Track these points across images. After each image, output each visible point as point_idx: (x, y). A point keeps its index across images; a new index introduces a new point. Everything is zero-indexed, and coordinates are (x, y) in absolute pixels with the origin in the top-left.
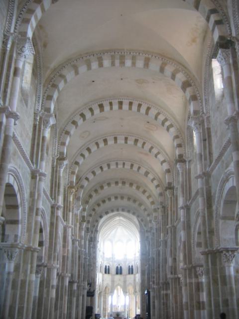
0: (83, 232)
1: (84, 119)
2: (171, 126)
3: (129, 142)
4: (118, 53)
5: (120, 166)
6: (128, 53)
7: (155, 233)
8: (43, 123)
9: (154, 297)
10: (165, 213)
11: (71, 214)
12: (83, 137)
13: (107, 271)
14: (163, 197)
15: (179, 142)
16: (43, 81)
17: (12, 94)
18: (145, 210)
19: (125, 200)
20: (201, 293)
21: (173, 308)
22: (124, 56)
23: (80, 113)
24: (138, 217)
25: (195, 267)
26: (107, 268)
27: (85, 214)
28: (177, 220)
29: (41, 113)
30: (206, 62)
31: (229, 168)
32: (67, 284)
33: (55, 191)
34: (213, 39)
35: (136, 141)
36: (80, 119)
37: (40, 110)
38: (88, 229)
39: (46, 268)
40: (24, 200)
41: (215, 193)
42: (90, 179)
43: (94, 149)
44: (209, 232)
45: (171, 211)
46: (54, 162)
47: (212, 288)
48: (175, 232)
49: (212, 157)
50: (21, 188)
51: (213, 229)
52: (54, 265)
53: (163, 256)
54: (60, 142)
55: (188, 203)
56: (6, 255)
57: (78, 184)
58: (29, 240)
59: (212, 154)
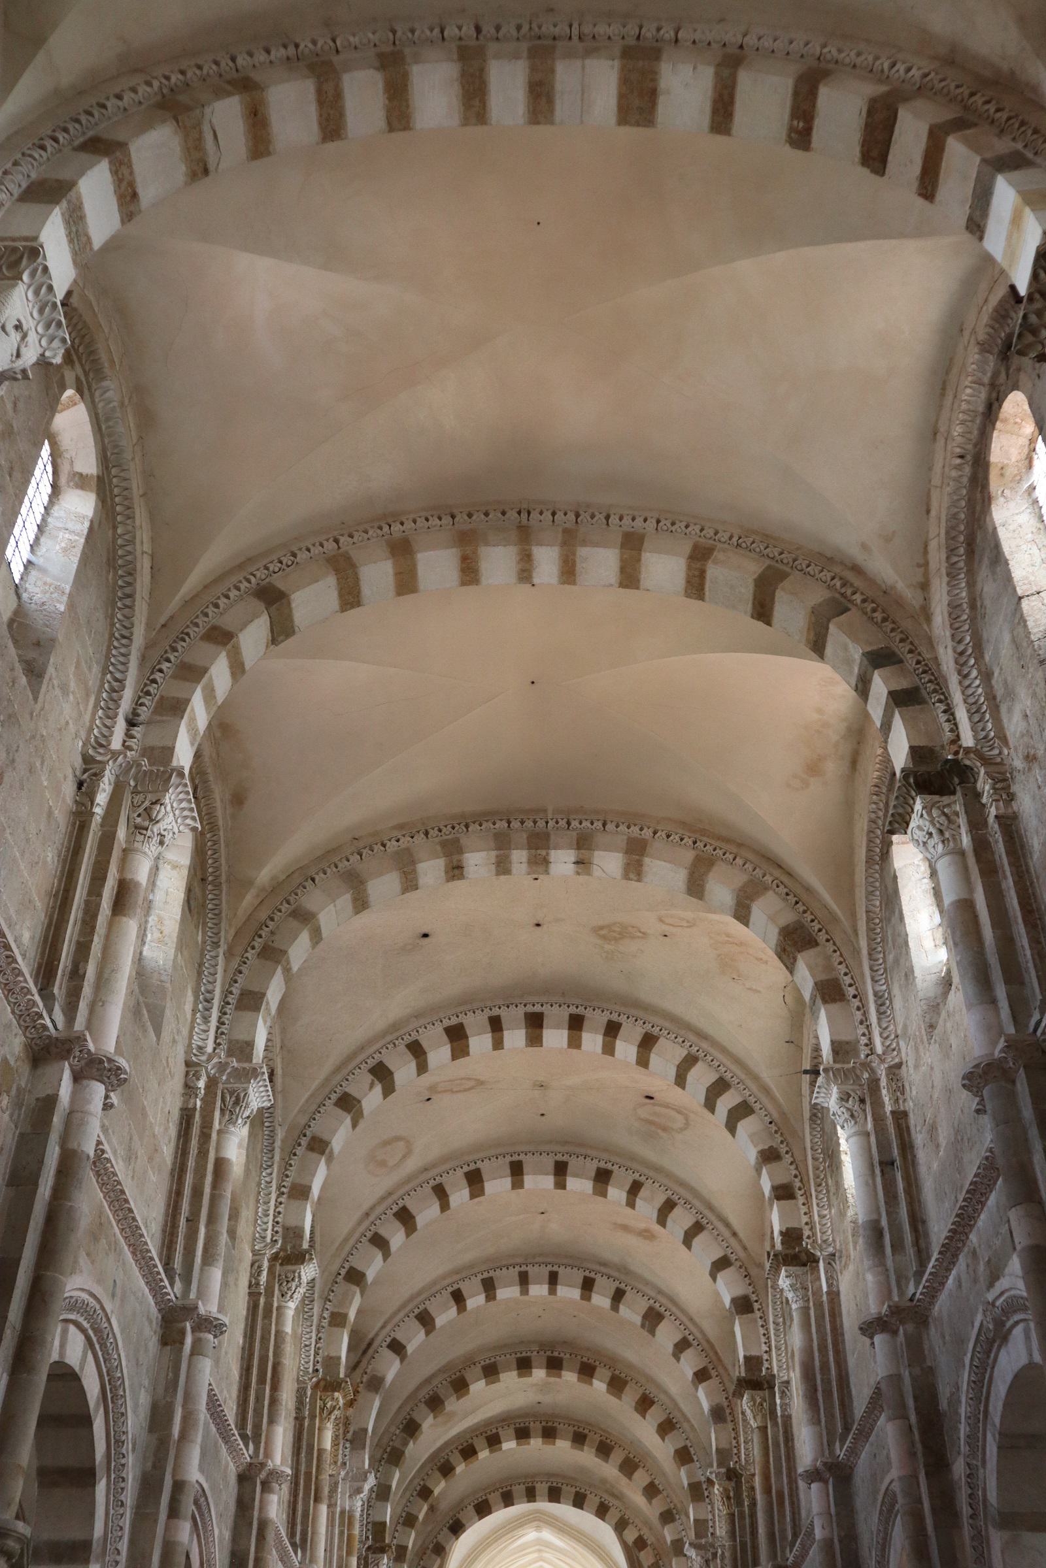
1: (389, 1090)
3: (572, 1183)
4: (522, 822)
5: (538, 1290)
6: (563, 823)
10: (740, 1503)
11: (323, 1509)
12: (383, 1164)
14: (730, 1426)
15: (782, 1179)
16: (227, 934)
17: (103, 983)
18: (651, 1491)
19: (563, 1446)
22: (547, 836)
23: (372, 1063)
24: (620, 1527)
27: (388, 1514)
28: (795, 1535)
29: (215, 1060)
30: (869, 850)
31: (1003, 1283)
33: (259, 1399)
34: (887, 760)
35: (602, 1177)
36: (372, 1086)
37: (209, 1049)
40: (120, 1443)
41: (954, 1401)
42: (410, 1349)
45: (767, 1490)
46: (259, 1275)
49: (927, 1235)
50: (114, 1389)
55: (841, 1452)
57: (359, 1371)
59: (924, 1222)
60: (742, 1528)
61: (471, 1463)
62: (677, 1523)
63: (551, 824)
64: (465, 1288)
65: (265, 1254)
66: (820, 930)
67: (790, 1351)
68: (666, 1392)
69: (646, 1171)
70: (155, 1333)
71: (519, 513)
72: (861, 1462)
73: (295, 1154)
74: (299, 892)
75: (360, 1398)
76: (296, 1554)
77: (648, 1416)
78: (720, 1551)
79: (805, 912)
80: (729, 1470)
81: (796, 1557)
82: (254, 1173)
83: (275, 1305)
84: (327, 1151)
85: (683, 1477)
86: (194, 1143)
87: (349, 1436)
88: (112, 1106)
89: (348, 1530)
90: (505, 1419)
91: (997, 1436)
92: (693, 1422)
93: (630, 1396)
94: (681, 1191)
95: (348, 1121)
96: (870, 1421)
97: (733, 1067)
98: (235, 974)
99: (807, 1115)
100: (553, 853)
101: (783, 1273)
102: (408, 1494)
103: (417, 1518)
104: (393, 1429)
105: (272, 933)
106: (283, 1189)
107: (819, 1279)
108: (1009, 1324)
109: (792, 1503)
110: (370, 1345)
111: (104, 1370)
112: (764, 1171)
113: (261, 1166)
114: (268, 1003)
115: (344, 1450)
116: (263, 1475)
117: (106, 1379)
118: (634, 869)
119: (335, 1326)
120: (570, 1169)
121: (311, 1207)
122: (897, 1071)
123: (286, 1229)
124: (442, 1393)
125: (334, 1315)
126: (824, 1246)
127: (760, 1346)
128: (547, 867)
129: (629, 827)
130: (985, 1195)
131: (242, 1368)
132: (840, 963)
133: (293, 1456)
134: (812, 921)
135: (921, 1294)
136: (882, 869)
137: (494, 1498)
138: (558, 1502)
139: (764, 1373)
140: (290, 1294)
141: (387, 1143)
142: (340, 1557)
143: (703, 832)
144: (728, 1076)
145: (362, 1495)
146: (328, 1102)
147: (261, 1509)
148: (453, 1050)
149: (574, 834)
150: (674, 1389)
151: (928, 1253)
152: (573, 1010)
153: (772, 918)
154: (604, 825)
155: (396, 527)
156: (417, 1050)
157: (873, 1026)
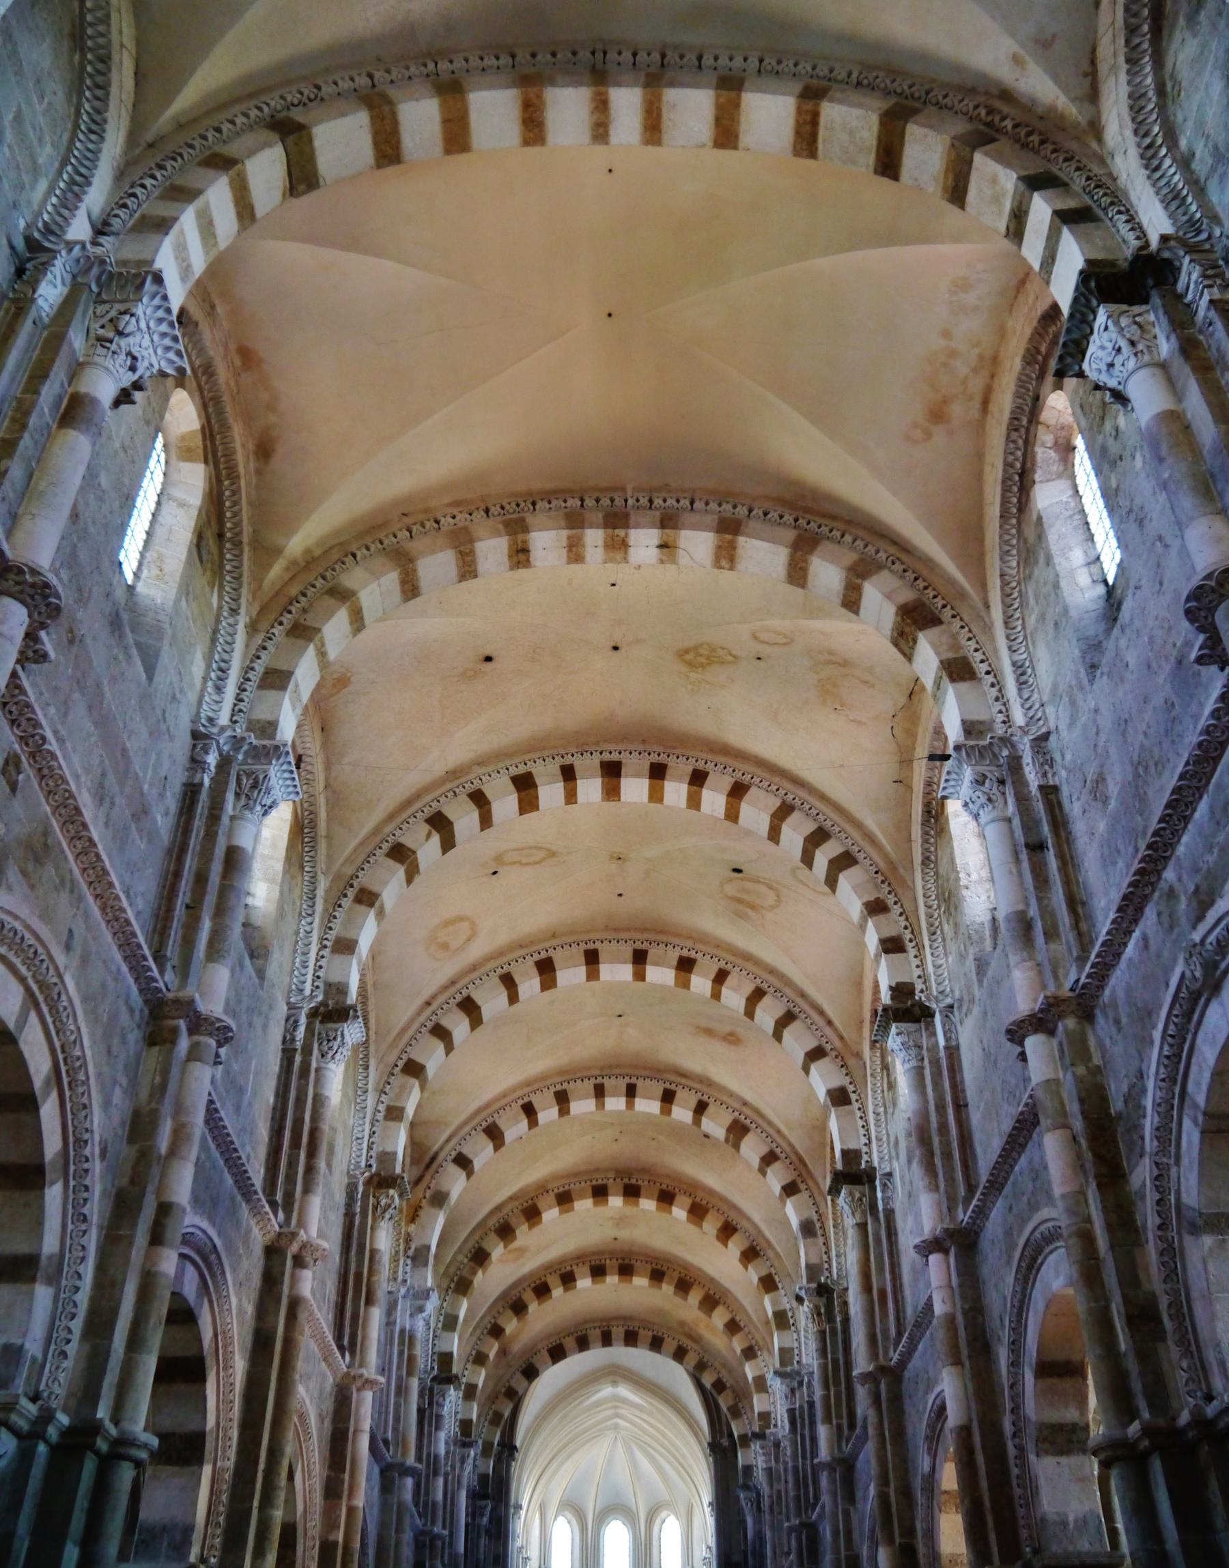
1: (448, 844)
2: (844, 861)
4: (598, 500)
5: (616, 1103)
6: (644, 501)
7: (786, 1444)
8: (232, 785)
10: (831, 1319)
14: (821, 1240)
15: (891, 932)
18: (733, 1327)
19: (640, 1281)
23: (428, 812)
28: (900, 1334)
33: (292, 1164)
35: (685, 965)
36: (429, 836)
38: (466, 1425)
40: (81, 1143)
41: (1134, 1096)
42: (477, 1164)
43: (492, 1002)
44: (1131, 1321)
45: (867, 1287)
48: (897, 1399)
49: (1090, 917)
51: (1152, 1300)
53: (836, 1551)
54: (332, 935)
55: (963, 1216)
60: (834, 1344)
61: (544, 1301)
62: (760, 1358)
63: (630, 502)
64: (536, 1100)
65: (301, 1008)
66: (944, 606)
67: (892, 1139)
68: (749, 1219)
69: (732, 959)
70: (139, 1026)
71: (593, 53)
72: (989, 1225)
73: (340, 906)
74: (337, 567)
75: (422, 1213)
77: (730, 1244)
78: (806, 1379)
79: (926, 588)
83: (314, 1065)
84: (377, 904)
86: (198, 823)
87: (410, 1253)
88: (43, 657)
89: (409, 1349)
90: (580, 1258)
91: (1200, 1118)
93: (711, 1225)
94: (772, 980)
95: (400, 872)
96: (1006, 1167)
97: (835, 817)
98: (257, 650)
99: (918, 859)
100: (633, 533)
102: (478, 1332)
104: (460, 1257)
105: (304, 611)
106: (325, 942)
107: (934, 1034)
109: (896, 1301)
110: (433, 1159)
111: (57, 1044)
112: (870, 924)
113: (300, 914)
114: (297, 686)
116: (294, 1248)
117: (61, 1057)
118: (726, 556)
120: (648, 960)
121: (359, 964)
122: (1043, 744)
123: (329, 985)
124: (513, 1222)
125: (390, 1109)
126: (941, 997)
127: (859, 1138)
128: (626, 553)
129: (720, 505)
130: (1192, 805)
131: (272, 1129)
132: (970, 639)
133: (342, 1253)
134: (935, 597)
135: (1088, 976)
136: (1019, 523)
137: (569, 1343)
138: (635, 1346)
139: (863, 1166)
140: (331, 1053)
142: (399, 1378)
143: (807, 510)
144: (829, 823)
145: (424, 1315)
146: (378, 852)
148: (520, 801)
149: (658, 514)
150: (756, 1217)
151: (1091, 937)
152: (654, 758)
153: (888, 596)
154: (692, 503)
155: (444, 66)
156: (479, 799)
157: (1012, 701)
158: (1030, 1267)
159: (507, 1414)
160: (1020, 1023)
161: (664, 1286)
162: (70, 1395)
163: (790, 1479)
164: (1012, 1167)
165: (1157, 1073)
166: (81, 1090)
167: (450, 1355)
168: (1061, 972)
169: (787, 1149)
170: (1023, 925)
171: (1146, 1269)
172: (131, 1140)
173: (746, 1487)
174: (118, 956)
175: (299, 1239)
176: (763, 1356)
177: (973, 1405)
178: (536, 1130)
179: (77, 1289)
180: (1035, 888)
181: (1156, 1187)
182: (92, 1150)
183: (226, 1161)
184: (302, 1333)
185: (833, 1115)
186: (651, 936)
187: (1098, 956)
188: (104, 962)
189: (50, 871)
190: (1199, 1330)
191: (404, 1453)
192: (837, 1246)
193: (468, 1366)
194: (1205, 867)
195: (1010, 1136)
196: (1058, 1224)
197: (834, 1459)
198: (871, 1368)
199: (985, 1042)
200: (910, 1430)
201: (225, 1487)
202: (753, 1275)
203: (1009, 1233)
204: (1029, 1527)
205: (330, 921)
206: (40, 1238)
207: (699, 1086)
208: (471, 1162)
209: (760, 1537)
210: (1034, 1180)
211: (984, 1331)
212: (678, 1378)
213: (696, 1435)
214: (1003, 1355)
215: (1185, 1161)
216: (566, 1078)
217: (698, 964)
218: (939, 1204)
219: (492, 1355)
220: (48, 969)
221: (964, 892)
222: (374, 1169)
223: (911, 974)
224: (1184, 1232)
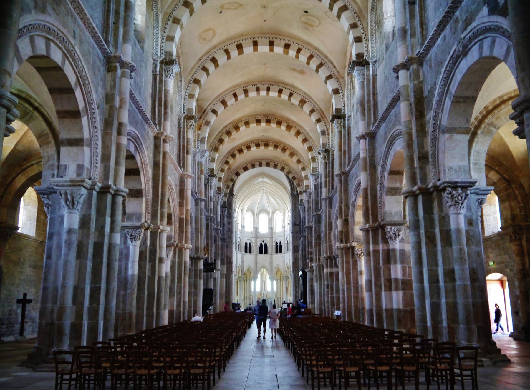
0: (212, 192)
2: (344, 8)
5: (263, 93)
7: (313, 194)
9: (312, 280)
10: (328, 159)
12: (205, 39)
13: (248, 249)
14: (327, 136)
15: (358, 35)
18: (299, 161)
19: (271, 148)
20: (392, 267)
21: (344, 290)
25: (383, 227)
26: (248, 245)
28: (349, 163)
32: (188, 259)
33: (160, 111)
35: (287, 46)
38: (219, 189)
39: (149, 232)
41: (431, 92)
42: (219, 113)
43: (222, 59)
44: (420, 159)
45: (340, 150)
46: (156, 68)
47: (424, 251)
48: (346, 181)
49: (427, 29)
51: (427, 153)
52: (161, 227)
54: (165, 35)
55: (372, 128)
56: (63, 202)
58: (106, 177)
59: (426, 24)
60: (329, 166)
62: (306, 170)
65: (158, 60)
68: (305, 130)
69: (303, 44)
70: (103, 65)
72: (380, 131)
73: (167, 24)
75: (202, 128)
76: (181, 169)
77: (299, 137)
80: (326, 149)
81: (349, 169)
82: (150, 28)
83: (164, 80)
84: (180, 23)
85: (310, 155)
87: (199, 139)
90: (252, 141)
91: (452, 98)
92: (313, 139)
93: (293, 131)
95: (187, 11)
96: (387, 113)
99: (370, 8)
101: (356, 69)
102: (221, 163)
103: (224, 170)
104: (215, 141)
106: (163, 37)
107: (369, 70)
108: (470, 46)
109: (349, 154)
110: (205, 111)
111: (77, 71)
112: (351, 32)
113: (154, 27)
115: (198, 144)
116: (163, 137)
117: (79, 75)
119: (190, 98)
120: (275, 44)
123: (166, 52)
124: (231, 130)
126: (372, 58)
131: (152, 100)
135: (423, 50)
137: (249, 166)
139: (342, 113)
141: (206, 31)
142: (198, 175)
146: (179, 4)
147: (163, 148)
150: (307, 129)
158: (391, 143)
159: (231, 185)
160: (398, 66)
161: (278, 150)
162: (100, 178)
163: (314, 203)
164: (389, 113)
165: (441, 83)
166: (87, 86)
167: (213, 169)
168: (414, 49)
169: (318, 108)
170: (404, 32)
171: (427, 144)
172: (107, 103)
173: (301, 205)
174: (92, 41)
175: (164, 134)
176: (307, 170)
177: (369, 182)
178: (237, 102)
179: (97, 148)
180: (410, 18)
181: (434, 119)
182: (95, 106)
183: (138, 110)
184: (168, 162)
185: (333, 97)
186: (275, 36)
187: (427, 43)
188: (88, 43)
189: (62, 8)
190: (439, 161)
191: (201, 195)
192: (332, 138)
193: (219, 172)
194: (470, 11)
195: (390, 103)
196: (401, 130)
197: (327, 197)
198: (339, 173)
199: (386, 73)
200: (349, 189)
201: (150, 203)
202: (306, 146)
203: (386, 134)
204: (381, 214)
205: (164, 30)
206: (83, 133)
207: (290, 88)
208: (217, 112)
209: (304, 217)
210: (396, 117)
211: (375, 162)
212: (282, 176)
213: (287, 191)
214: (379, 169)
215: (444, 111)
216: (247, 85)
217: (291, 46)
218: (365, 125)
219: (226, 169)
220: (69, 45)
221: (385, 20)
222: (186, 114)
223: (363, 50)
224: (440, 133)
